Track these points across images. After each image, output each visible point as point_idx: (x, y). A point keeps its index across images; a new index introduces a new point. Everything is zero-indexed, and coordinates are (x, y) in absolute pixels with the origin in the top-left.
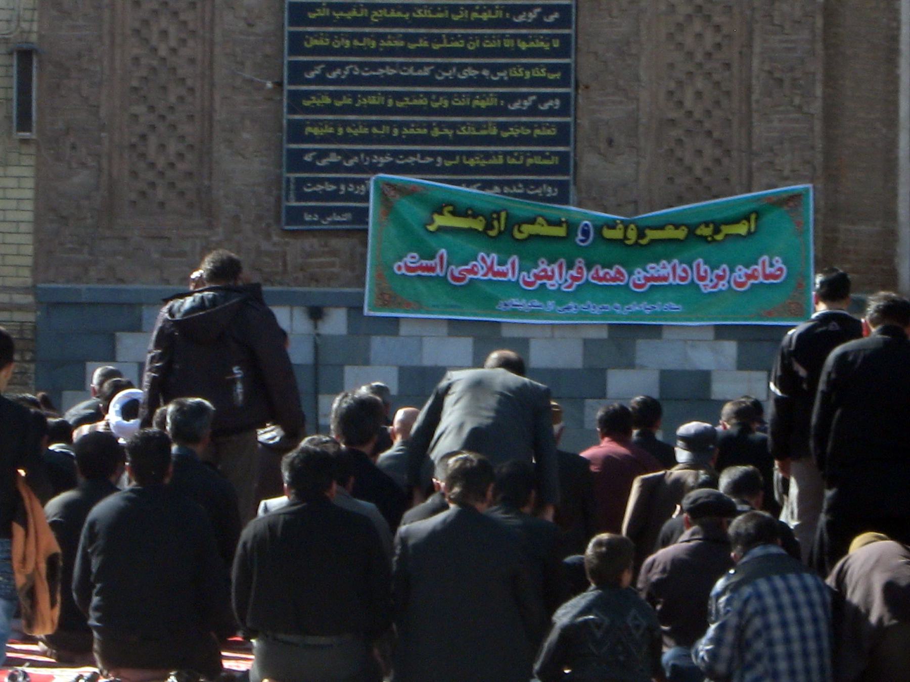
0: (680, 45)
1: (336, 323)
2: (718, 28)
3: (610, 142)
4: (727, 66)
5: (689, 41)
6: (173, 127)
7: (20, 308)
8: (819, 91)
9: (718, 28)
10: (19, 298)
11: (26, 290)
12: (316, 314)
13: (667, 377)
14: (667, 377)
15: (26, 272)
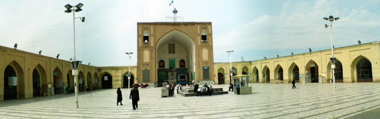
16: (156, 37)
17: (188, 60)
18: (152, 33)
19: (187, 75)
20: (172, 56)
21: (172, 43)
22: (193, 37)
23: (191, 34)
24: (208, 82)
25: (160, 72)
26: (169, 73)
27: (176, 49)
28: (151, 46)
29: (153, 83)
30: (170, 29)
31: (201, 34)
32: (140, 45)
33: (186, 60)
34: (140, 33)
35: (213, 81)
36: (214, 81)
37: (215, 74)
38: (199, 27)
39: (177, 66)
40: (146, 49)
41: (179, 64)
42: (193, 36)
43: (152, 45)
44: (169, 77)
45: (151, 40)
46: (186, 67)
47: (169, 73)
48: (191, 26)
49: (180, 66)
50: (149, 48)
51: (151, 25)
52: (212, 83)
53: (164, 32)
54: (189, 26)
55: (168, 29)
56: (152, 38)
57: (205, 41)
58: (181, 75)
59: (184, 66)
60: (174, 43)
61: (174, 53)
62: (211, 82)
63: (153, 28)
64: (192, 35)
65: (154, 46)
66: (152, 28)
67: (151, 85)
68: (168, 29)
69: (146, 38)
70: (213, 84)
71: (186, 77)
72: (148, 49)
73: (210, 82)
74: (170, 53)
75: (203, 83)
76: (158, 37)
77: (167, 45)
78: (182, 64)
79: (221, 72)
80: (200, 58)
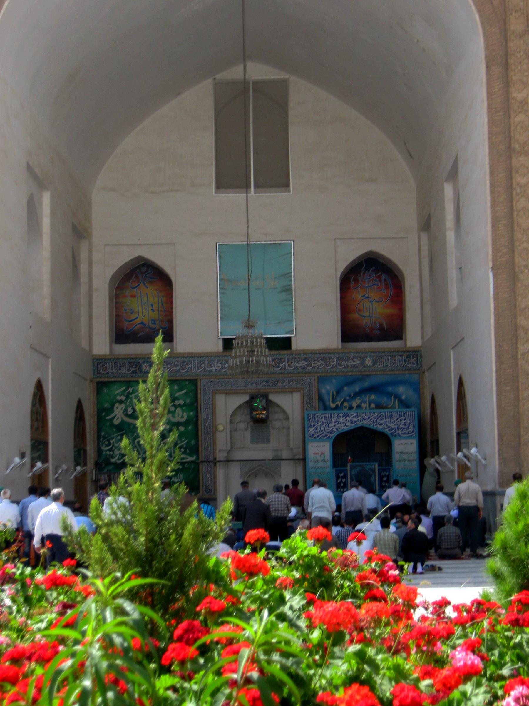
17: (435, 260)
19: (413, 428)
20: (263, 215)
21: (258, 71)
25: (118, 391)
26: (220, 400)
27: (299, 137)
33: (405, 254)
39: (316, 327)
41: (331, 295)
44: (222, 441)
46: (413, 338)
47: (226, 407)
49: (350, 332)
58: (344, 423)
59: (394, 330)
60: (287, 76)
61: (276, 178)
71: (405, 448)
74: (229, 177)
77: (198, 100)
78: (372, 307)
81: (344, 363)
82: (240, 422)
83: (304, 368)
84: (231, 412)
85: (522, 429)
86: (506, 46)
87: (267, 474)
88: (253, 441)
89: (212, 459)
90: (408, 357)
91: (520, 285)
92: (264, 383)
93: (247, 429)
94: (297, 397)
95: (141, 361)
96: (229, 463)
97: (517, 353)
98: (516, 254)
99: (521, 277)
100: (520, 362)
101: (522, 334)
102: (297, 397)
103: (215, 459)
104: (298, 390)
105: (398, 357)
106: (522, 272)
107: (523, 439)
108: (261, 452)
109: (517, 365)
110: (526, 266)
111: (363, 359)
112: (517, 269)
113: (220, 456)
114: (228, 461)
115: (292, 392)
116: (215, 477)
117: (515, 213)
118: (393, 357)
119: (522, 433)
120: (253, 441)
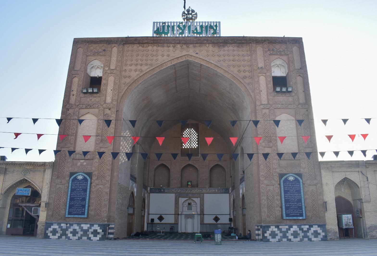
0: (98, 203)
1: (68, 225)
2: (101, 201)
3: (91, 210)
4: (101, 204)
5: (98, 202)
6: (58, 209)
7: (44, 223)
8: (108, 206)
9: (101, 201)
10: (44, 223)
11: (45, 222)
12: (67, 224)
13: (94, 230)
14: (94, 230)
15: (45, 221)
16: (125, 77)
18: (112, 67)
22: (245, 77)
23: (235, 70)
24: (301, 229)
28: (105, 103)
29: (99, 225)
30: (168, 55)
31: (270, 70)
32: (73, 99)
34: (78, 67)
35: (319, 226)
36: (322, 226)
37: (326, 199)
38: (259, 50)
40: (90, 110)
42: (242, 74)
43: (109, 100)
45: (106, 85)
48: (235, 48)
50: (98, 108)
51: (113, 45)
52: (316, 234)
53: (149, 62)
54: (231, 48)
55: (163, 55)
56: (111, 79)
57: (284, 89)
62: (312, 229)
63: (119, 52)
64: (239, 71)
65: (115, 103)
66: (115, 50)
67: (71, 230)
68: (163, 55)
69: (96, 82)
70: (320, 237)
72: (97, 110)
73: (309, 229)
75: (281, 232)
76: (130, 77)
79: (346, 194)
80: (271, 144)
81: (211, 191)
82: (185, 205)
83: (201, 192)
84: (183, 202)
85: (261, 208)
86: (256, 108)
87: (191, 218)
88: (188, 210)
89: (177, 214)
90: (226, 190)
91: (260, 169)
92: (191, 195)
93: (186, 207)
94: (199, 199)
95: (161, 189)
96: (182, 215)
97: (260, 187)
98: (259, 161)
99: (261, 167)
100: (261, 189)
101: (261, 182)
102: (199, 199)
103: (178, 214)
104: (199, 197)
105: (224, 190)
106: (261, 165)
107: (262, 211)
108: (189, 212)
109: (260, 190)
110: (262, 164)
111: (215, 190)
112: (259, 164)
113: (180, 213)
114: (181, 214)
115: (198, 198)
116: (178, 218)
117: (259, 150)
118: (223, 190)
119: (262, 209)
120: (188, 210)
